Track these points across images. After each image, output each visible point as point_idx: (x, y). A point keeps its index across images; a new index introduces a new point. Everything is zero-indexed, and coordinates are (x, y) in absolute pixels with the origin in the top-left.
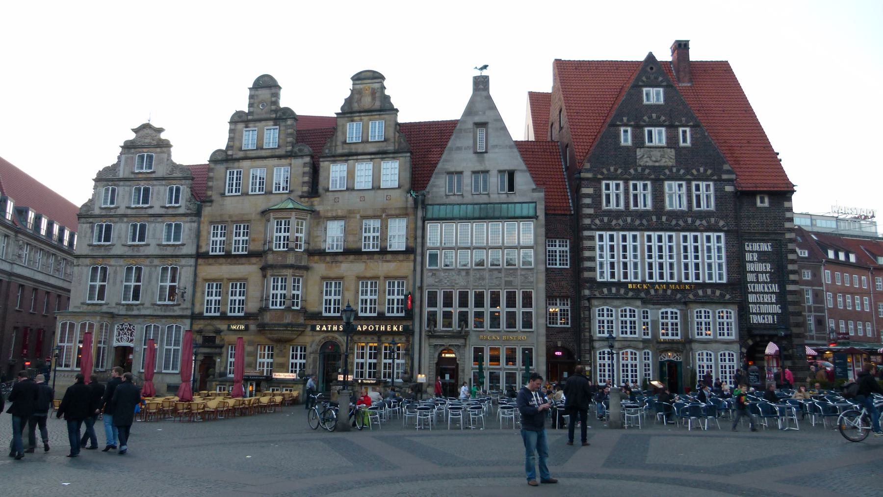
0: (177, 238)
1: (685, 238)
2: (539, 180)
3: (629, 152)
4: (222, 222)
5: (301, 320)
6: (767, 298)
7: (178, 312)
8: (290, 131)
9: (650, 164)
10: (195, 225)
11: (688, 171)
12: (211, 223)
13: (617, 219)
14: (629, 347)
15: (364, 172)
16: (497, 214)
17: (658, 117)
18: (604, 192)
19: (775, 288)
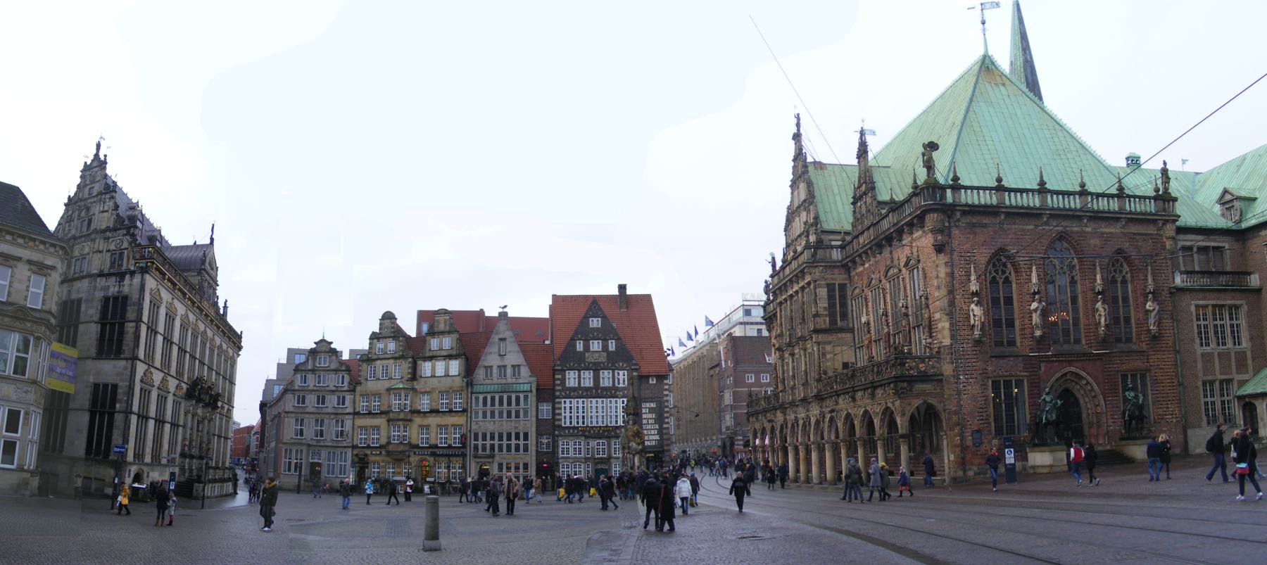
0: (343, 404)
1: (611, 401)
2: (533, 371)
3: (582, 354)
4: (366, 395)
5: (407, 448)
6: (653, 432)
7: (346, 445)
8: (401, 344)
9: (593, 361)
10: (352, 396)
11: (613, 365)
12: (361, 395)
13: (574, 392)
14: (578, 462)
15: (440, 367)
16: (511, 390)
17: (598, 335)
18: (567, 377)
19: (657, 427)
